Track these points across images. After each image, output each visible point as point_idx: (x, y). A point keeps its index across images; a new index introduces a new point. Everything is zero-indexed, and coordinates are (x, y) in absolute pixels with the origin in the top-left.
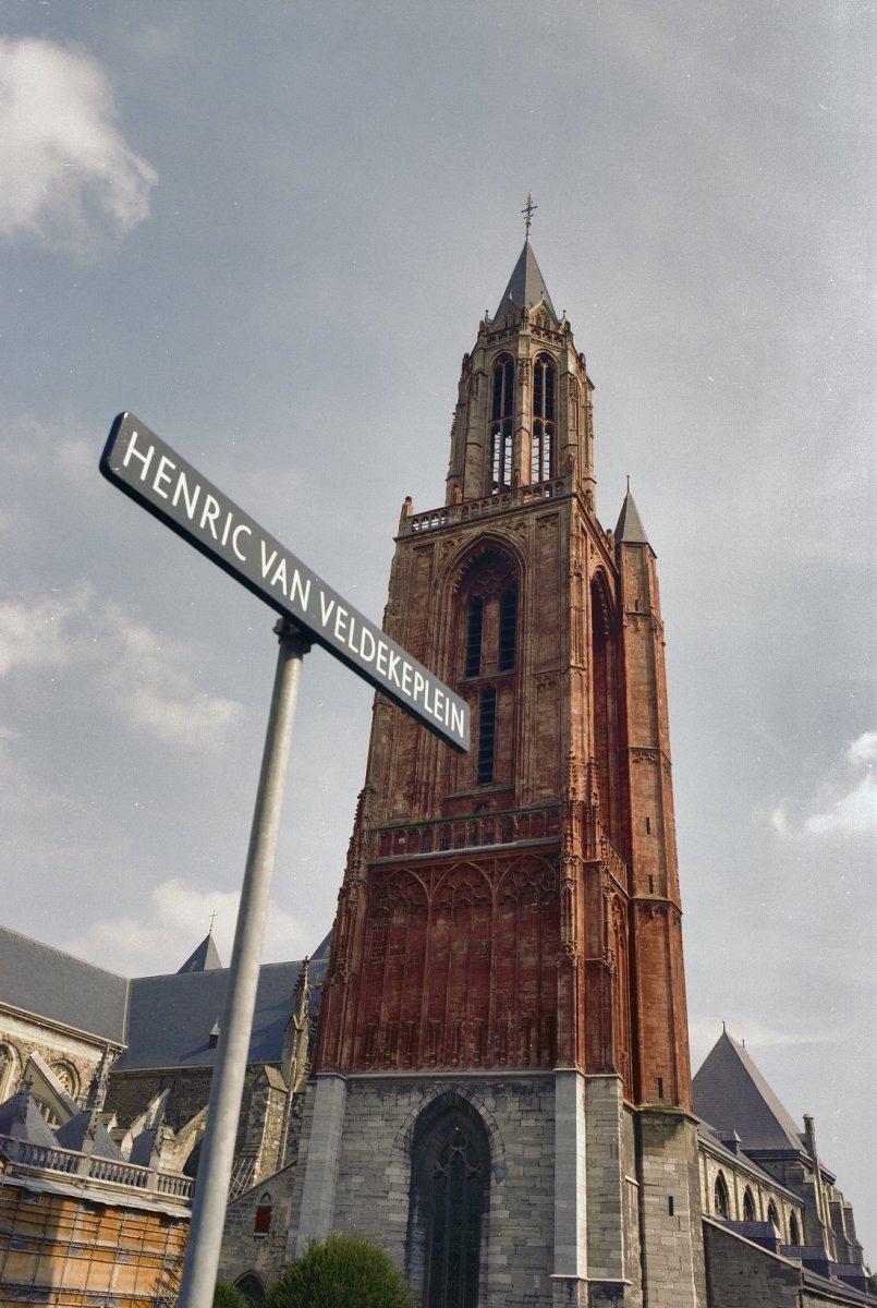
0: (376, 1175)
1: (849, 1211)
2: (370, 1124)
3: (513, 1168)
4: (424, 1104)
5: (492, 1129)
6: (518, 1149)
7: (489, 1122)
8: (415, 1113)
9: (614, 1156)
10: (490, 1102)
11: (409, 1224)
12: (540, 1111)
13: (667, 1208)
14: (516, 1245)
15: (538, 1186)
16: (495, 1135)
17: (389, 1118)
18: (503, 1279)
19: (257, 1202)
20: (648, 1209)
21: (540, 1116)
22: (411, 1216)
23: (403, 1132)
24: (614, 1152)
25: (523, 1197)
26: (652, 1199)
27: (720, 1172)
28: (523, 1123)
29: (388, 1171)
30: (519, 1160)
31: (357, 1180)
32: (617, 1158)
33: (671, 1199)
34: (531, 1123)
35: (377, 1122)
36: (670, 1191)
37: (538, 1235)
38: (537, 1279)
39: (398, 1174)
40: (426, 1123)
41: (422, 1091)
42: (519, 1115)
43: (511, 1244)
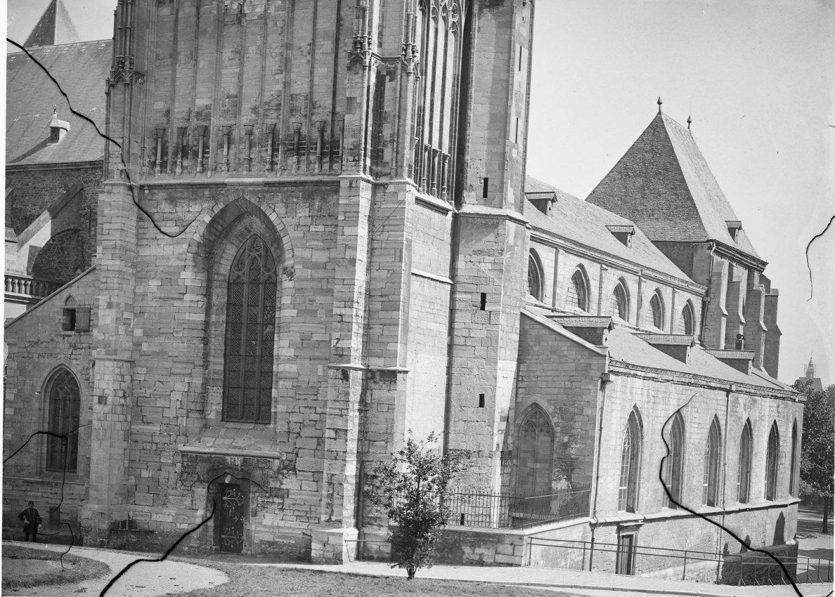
0: (170, 278)
1: (773, 300)
3: (300, 271)
4: (216, 210)
6: (307, 254)
7: (279, 228)
8: (207, 219)
9: (398, 259)
10: (281, 209)
11: (207, 324)
13: (479, 304)
14: (302, 340)
15: (325, 287)
16: (285, 240)
18: (291, 368)
20: (458, 305)
22: (208, 315)
23: (197, 237)
24: (398, 255)
26: (464, 296)
27: (581, 266)
28: (312, 229)
29: (184, 275)
30: (308, 264)
31: (154, 283)
32: (401, 261)
33: (483, 296)
36: (483, 289)
37: (323, 331)
38: (320, 368)
40: (219, 230)
41: (214, 198)
42: (309, 221)
43: (298, 339)
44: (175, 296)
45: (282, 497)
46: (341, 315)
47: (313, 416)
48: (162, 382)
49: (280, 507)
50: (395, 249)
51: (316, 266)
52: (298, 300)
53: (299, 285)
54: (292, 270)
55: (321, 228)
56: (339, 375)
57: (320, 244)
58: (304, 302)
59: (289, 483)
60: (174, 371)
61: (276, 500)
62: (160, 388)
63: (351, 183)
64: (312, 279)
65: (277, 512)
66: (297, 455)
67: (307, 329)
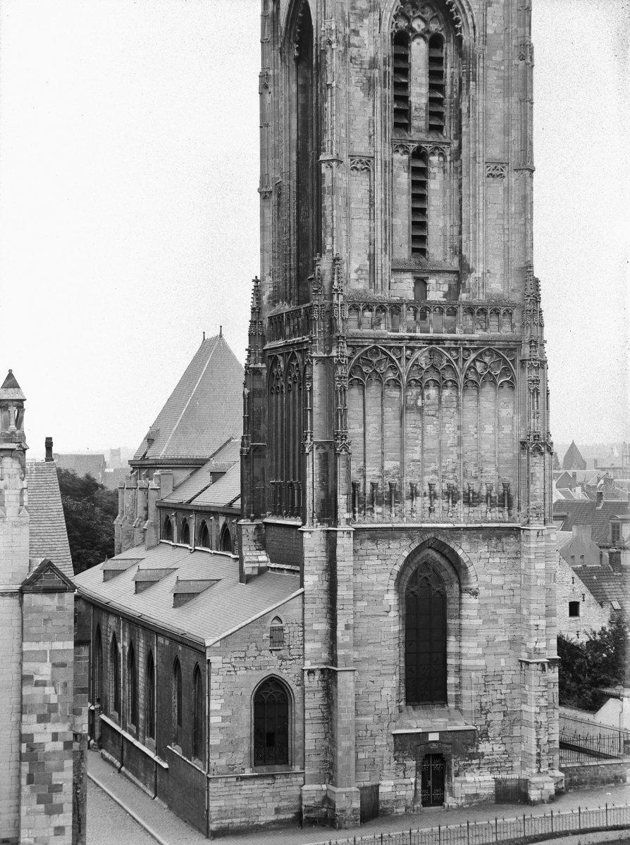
0: (378, 599)
2: (367, 562)
3: (483, 592)
5: (468, 565)
6: (488, 579)
8: (406, 554)
10: (466, 546)
12: (503, 551)
16: (471, 569)
17: (384, 558)
19: (269, 625)
21: (503, 556)
25: (492, 610)
28: (491, 560)
29: (387, 596)
30: (488, 586)
34: (497, 560)
35: (374, 561)
38: (503, 661)
39: (391, 598)
41: (411, 538)
42: (488, 555)
44: (383, 614)
45: (479, 758)
46: (537, 626)
47: (499, 696)
48: (373, 682)
49: (478, 766)
50: (551, 574)
51: (496, 587)
52: (483, 613)
53: (483, 602)
54: (477, 591)
55: (497, 560)
56: (539, 667)
57: (498, 571)
58: (488, 613)
59: (484, 747)
60: (383, 672)
61: (474, 762)
62: (372, 687)
63: (538, 533)
64: (493, 597)
65: (475, 770)
66: (489, 726)
67: (491, 633)
